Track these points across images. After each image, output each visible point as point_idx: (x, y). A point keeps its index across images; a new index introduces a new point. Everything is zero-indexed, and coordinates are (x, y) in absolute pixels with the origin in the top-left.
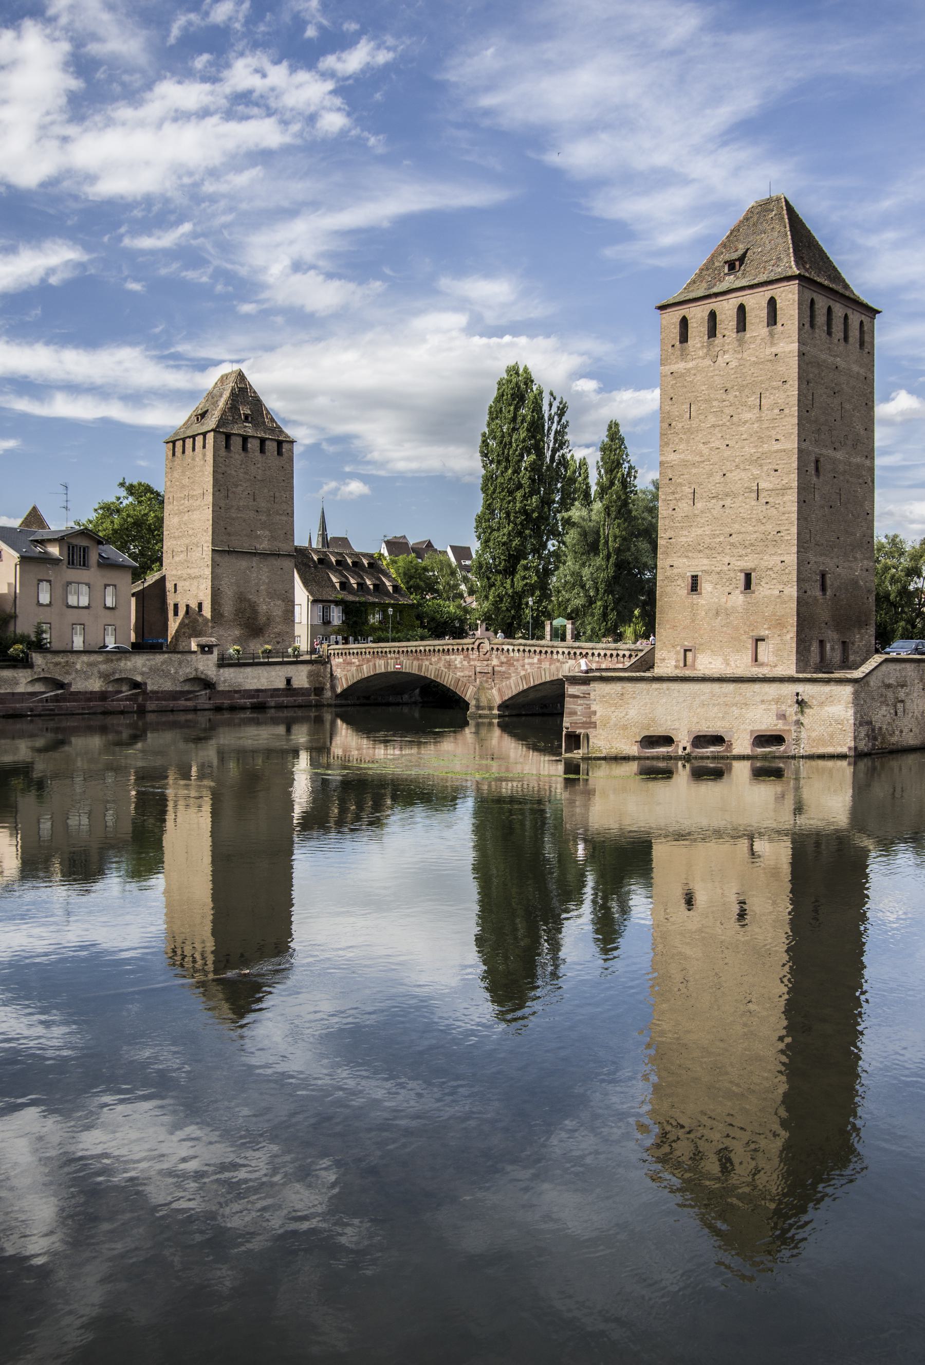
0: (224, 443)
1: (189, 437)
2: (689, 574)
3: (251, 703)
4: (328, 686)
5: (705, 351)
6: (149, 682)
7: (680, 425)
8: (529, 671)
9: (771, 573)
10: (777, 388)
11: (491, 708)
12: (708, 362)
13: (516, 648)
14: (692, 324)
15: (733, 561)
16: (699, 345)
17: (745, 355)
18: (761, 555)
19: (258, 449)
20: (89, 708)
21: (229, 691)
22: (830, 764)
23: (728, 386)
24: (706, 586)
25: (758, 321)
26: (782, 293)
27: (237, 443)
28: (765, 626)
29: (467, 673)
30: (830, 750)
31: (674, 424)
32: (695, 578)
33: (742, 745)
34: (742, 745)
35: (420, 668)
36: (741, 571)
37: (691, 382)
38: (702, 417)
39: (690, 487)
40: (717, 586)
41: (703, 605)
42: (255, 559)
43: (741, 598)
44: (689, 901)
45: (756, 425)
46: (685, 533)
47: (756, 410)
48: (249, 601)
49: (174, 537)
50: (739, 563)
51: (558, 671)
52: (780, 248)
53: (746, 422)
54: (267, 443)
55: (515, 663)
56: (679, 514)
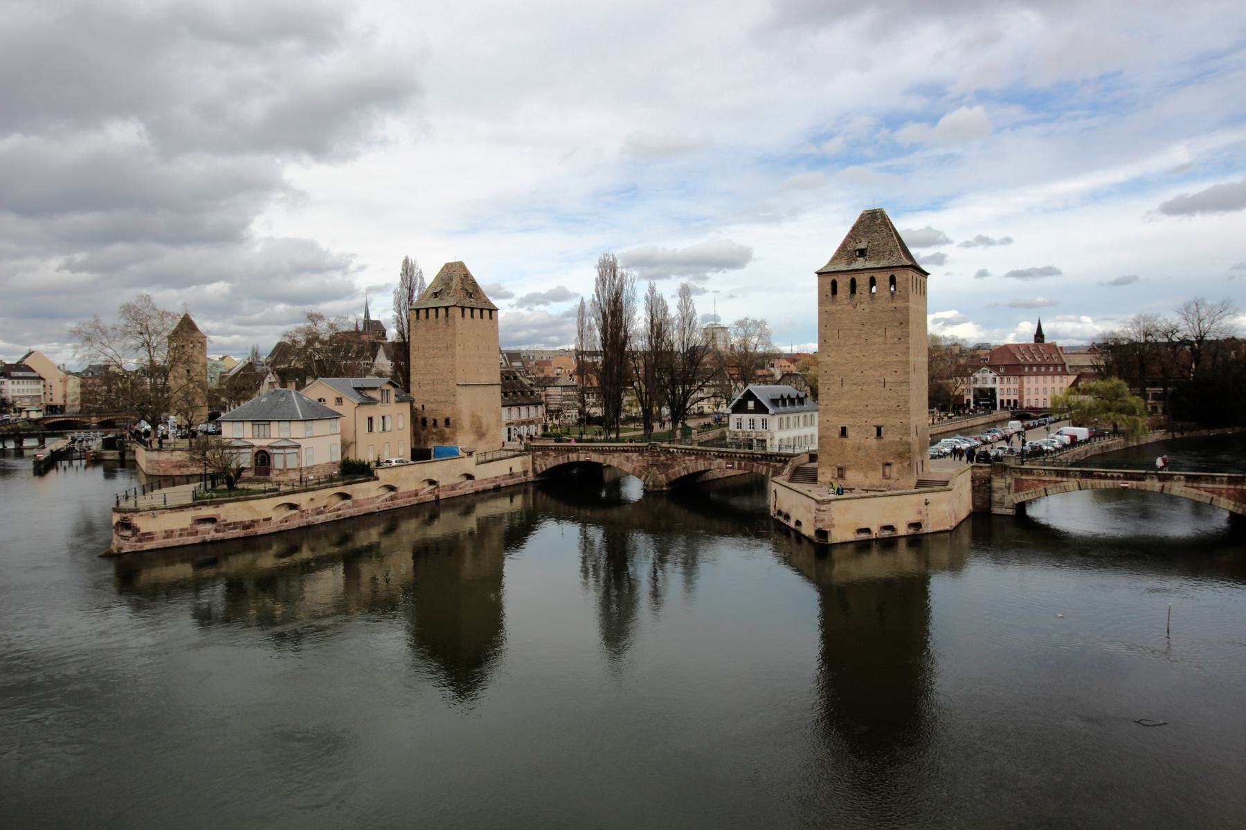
0: (461, 314)
2: (840, 426)
3: (494, 486)
4: (531, 469)
5: (848, 301)
6: (440, 480)
7: (832, 342)
9: (894, 428)
10: (896, 326)
11: (662, 487)
12: (850, 307)
13: (679, 451)
14: (839, 285)
16: (844, 297)
17: (875, 306)
19: (479, 316)
20: (410, 502)
21: (482, 480)
22: (942, 535)
23: (864, 322)
24: (850, 433)
27: (468, 312)
29: (641, 464)
30: (941, 528)
31: (828, 340)
33: (902, 530)
34: (902, 530)
35: (605, 460)
36: (875, 426)
37: (839, 318)
38: (847, 338)
40: (860, 434)
41: (849, 444)
42: (480, 388)
43: (875, 441)
45: (882, 346)
46: (836, 403)
47: (883, 338)
48: (477, 416)
50: (874, 422)
51: (710, 464)
52: (890, 244)
53: (875, 344)
54: (484, 311)
55: (678, 459)
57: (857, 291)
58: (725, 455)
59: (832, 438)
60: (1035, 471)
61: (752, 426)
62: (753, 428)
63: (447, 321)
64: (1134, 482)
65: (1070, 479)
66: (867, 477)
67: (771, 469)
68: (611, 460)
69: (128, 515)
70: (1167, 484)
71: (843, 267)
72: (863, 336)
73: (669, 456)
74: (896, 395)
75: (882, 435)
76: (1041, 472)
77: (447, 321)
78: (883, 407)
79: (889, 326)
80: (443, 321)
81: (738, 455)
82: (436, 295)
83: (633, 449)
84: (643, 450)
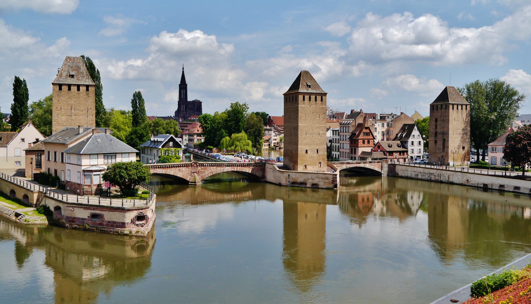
1: (75, 85)
8: (213, 170)
11: (200, 182)
12: (309, 106)
15: (315, 147)
16: (307, 102)
24: (309, 152)
29: (188, 172)
32: (307, 151)
38: (308, 117)
44: (306, 216)
45: (319, 121)
47: (319, 118)
49: (63, 125)
53: (316, 120)
56: (303, 137)
58: (231, 165)
59: (303, 154)
60: (336, 163)
63: (88, 94)
64: (358, 164)
66: (314, 168)
69: (144, 210)
70: (366, 164)
71: (305, 91)
75: (318, 152)
76: (337, 163)
77: (88, 94)
78: (318, 142)
80: (84, 93)
81: (237, 165)
82: (72, 76)
83: (184, 165)
84: (189, 165)
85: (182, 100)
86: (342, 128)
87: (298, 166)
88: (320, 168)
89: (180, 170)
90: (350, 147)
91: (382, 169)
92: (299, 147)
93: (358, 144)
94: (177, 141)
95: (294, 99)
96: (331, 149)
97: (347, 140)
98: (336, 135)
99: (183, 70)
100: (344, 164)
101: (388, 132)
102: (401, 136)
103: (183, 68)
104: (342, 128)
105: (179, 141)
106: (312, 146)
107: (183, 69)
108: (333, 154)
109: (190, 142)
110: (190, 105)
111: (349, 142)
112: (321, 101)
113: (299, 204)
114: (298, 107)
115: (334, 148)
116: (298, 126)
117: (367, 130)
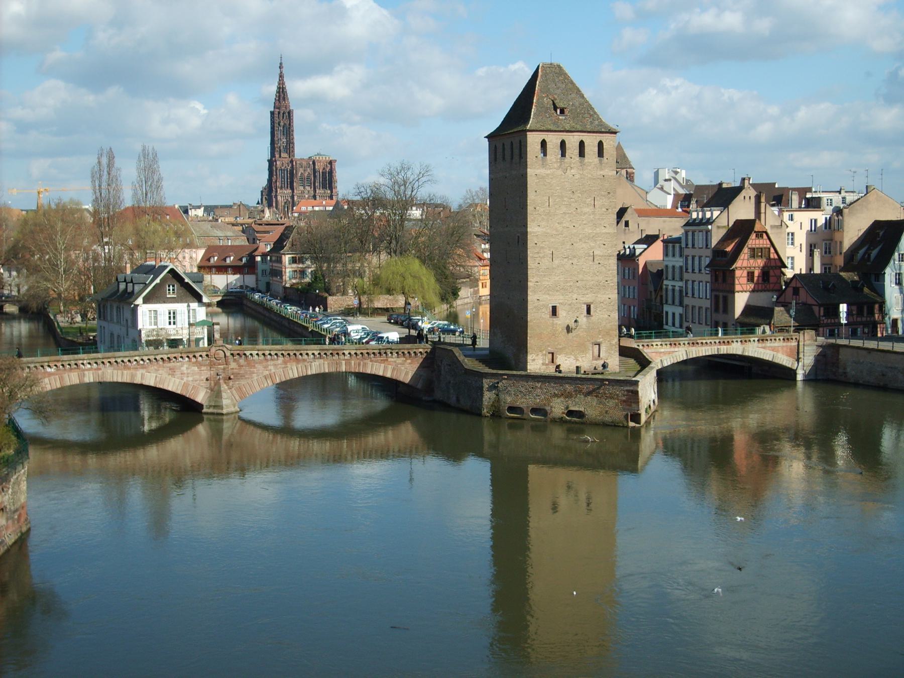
2: (551, 305)
7: (542, 210)
8: (273, 371)
9: (602, 304)
10: (604, 196)
16: (554, 160)
18: (596, 295)
23: (574, 190)
25: (592, 153)
26: (607, 139)
28: (600, 336)
29: (197, 377)
31: (538, 208)
35: (133, 376)
36: (585, 303)
38: (557, 206)
39: (550, 250)
43: (585, 319)
44: (555, 508)
45: (592, 216)
50: (582, 299)
53: (585, 214)
57: (567, 156)
60: (654, 344)
61: (172, 320)
62: (174, 323)
64: (725, 347)
65: (680, 349)
66: (577, 360)
67: (390, 366)
68: (143, 376)
72: (573, 204)
73: (242, 361)
74: (604, 269)
75: (592, 313)
79: (598, 196)
85: (280, 157)
86: (690, 234)
87: (530, 357)
88: (596, 360)
89: (172, 372)
90: (714, 293)
91: (798, 360)
92: (532, 297)
93: (733, 284)
94: (188, 283)
95: (516, 151)
96: (661, 296)
97: (703, 271)
98: (674, 255)
99: (281, 73)
100: (680, 344)
101: (830, 244)
102: (867, 256)
103: (281, 64)
104: (690, 234)
105: (194, 282)
106: (570, 295)
107: (281, 67)
108: (667, 313)
109: (274, 279)
110: (301, 171)
111: (708, 278)
112: (599, 156)
113: (532, 468)
114: (524, 176)
115: (670, 294)
116: (527, 232)
117: (761, 241)
